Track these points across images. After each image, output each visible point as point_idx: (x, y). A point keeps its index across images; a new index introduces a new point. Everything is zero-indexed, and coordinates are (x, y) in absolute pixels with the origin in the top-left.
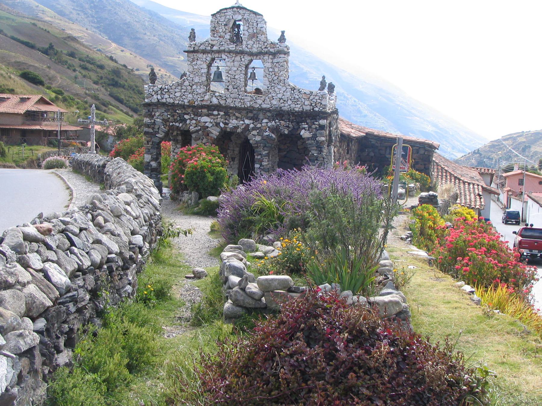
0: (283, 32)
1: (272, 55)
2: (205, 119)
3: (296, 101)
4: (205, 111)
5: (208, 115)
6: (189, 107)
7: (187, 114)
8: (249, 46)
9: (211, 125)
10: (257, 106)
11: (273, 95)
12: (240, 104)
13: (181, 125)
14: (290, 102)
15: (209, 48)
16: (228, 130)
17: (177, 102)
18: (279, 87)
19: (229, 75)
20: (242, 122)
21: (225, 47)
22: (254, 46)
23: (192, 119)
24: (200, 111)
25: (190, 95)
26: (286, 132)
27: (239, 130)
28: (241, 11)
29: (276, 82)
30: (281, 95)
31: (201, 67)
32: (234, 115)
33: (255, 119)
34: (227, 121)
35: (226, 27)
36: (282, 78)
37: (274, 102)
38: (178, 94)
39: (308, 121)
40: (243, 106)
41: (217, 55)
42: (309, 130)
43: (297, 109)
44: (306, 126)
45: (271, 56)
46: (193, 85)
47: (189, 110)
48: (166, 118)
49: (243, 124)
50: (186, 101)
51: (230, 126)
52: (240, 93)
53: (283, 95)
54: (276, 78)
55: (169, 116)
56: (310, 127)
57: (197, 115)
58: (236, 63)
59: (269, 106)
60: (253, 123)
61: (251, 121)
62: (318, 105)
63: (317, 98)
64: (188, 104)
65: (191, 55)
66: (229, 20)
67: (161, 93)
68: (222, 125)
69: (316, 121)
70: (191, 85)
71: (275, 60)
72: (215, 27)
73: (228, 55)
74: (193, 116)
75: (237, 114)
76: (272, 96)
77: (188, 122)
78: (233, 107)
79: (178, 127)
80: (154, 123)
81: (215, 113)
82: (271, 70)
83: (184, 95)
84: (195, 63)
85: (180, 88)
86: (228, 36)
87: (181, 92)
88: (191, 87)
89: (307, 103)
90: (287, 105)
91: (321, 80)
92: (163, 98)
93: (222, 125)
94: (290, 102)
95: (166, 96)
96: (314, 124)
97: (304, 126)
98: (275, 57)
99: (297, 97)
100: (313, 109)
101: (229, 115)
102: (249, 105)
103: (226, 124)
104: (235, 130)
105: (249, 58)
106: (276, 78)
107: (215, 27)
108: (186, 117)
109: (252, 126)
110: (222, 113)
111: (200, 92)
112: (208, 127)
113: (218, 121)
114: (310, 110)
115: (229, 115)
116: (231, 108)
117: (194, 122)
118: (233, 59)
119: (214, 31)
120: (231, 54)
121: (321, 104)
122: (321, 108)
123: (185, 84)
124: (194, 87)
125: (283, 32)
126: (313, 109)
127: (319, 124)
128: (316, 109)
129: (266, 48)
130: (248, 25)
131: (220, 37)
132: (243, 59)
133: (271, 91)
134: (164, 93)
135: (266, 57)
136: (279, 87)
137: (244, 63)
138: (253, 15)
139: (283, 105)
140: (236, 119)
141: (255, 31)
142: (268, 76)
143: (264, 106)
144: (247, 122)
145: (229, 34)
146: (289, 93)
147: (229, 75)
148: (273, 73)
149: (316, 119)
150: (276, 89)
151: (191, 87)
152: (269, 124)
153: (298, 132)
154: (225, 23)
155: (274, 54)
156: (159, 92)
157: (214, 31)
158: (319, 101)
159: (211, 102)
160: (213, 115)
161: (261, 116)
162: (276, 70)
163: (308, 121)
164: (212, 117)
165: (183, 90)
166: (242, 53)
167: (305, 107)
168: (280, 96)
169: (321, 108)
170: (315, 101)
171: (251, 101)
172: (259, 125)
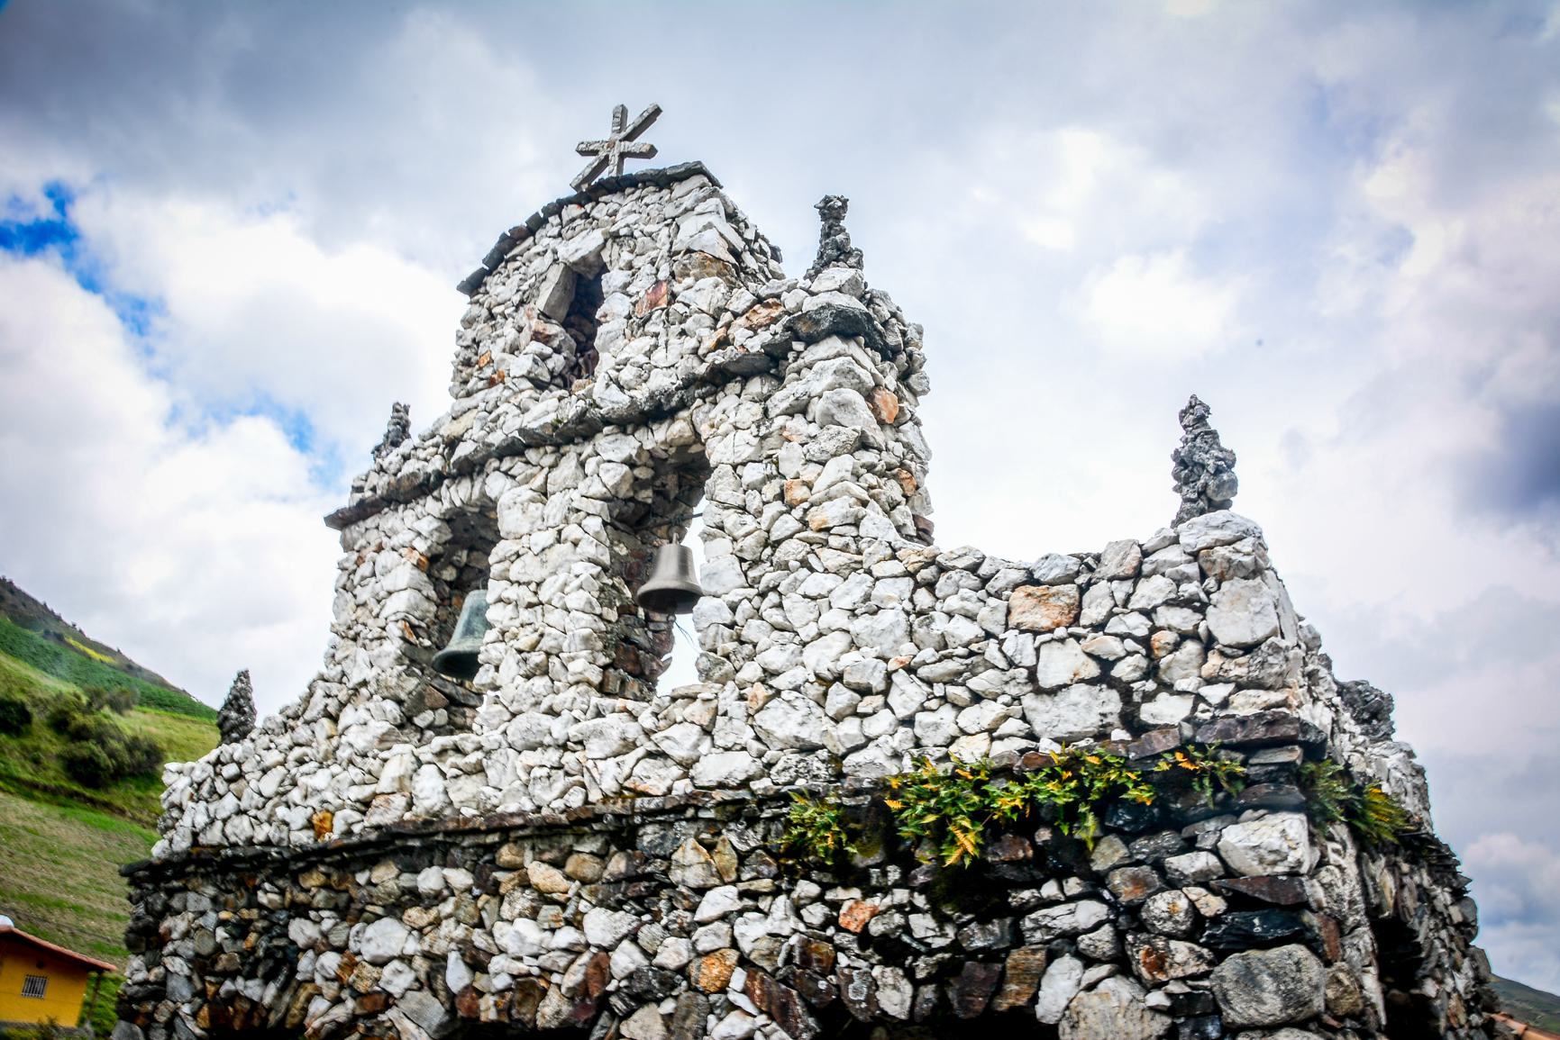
0: (832, 212)
1: (762, 373)
2: (385, 937)
3: (957, 677)
4: (386, 876)
5: (395, 908)
6: (310, 858)
7: (301, 910)
8: (627, 375)
9: (407, 979)
10: (658, 780)
11: (774, 658)
12: (560, 782)
13: (272, 989)
14: (908, 694)
15: (437, 464)
16: (488, 1010)
17: (260, 836)
18: (815, 583)
19: (512, 592)
20: (567, 936)
21: (511, 425)
22: (658, 356)
23: (317, 948)
24: (361, 878)
25: (321, 780)
26: (895, 998)
27: (552, 1009)
28: (600, 212)
29: (791, 550)
30: (838, 642)
31: (387, 583)
32: (525, 884)
33: (645, 891)
34: (479, 938)
35: (521, 318)
36: (831, 513)
37: (784, 721)
38: (269, 785)
39: (1107, 854)
40: (575, 799)
41: (458, 494)
42: (1122, 965)
43: (971, 751)
44: (1090, 912)
45: (756, 386)
46: (342, 705)
47: (313, 880)
48: (207, 948)
49: (573, 951)
50: (297, 817)
51: (500, 973)
52: (556, 701)
53: (854, 645)
54: (789, 523)
55: (221, 933)
56: (1129, 918)
57: (349, 912)
58: (556, 505)
59: (741, 765)
60: (633, 937)
61: (624, 921)
62: (1184, 667)
63: (1152, 590)
64: (305, 838)
65: (355, 531)
66: (542, 277)
67: (213, 791)
68: (456, 975)
69: (1190, 845)
70: (331, 709)
71: (781, 399)
72: (476, 342)
73: (519, 468)
74: (327, 925)
75: (540, 874)
76: (769, 674)
77: (304, 963)
78: (521, 814)
79: (255, 1005)
80: (158, 991)
81: (429, 880)
82: (752, 473)
83: (295, 784)
84: (365, 569)
85: (285, 741)
86: (520, 365)
87: (283, 764)
88: (335, 719)
89: (1061, 663)
90: (880, 724)
91: (1175, 437)
92: (212, 821)
93: (456, 975)
94: (908, 694)
95: (229, 803)
96: (1172, 882)
97: (1061, 918)
98: (780, 379)
99: (964, 631)
100: (1130, 720)
101: (494, 890)
102: (609, 785)
103: (477, 963)
104: (524, 1013)
105: (628, 446)
106: (789, 523)
107: (476, 342)
108: (301, 931)
109: (625, 960)
110: (461, 878)
111: (360, 744)
112: (388, 1001)
113: (440, 947)
114: (1102, 735)
115: (494, 890)
116: (505, 830)
117: (331, 961)
118: (539, 481)
119: (467, 363)
120: (531, 455)
121: (1209, 643)
122: (1215, 693)
123: (308, 716)
124: (347, 717)
125: (832, 212)
126: (1130, 720)
127: (1225, 878)
128: (1166, 711)
129: (723, 343)
130: (626, 256)
131: (491, 383)
132: (590, 466)
133: (752, 630)
134: (221, 786)
135: (728, 400)
136: (815, 583)
137: (597, 489)
138: (657, 196)
139: (850, 727)
140: (534, 914)
141: (663, 274)
142: (731, 519)
143: (713, 768)
144: (601, 925)
145: (537, 347)
146: (892, 617)
147: (512, 592)
148: (771, 490)
149: (1176, 822)
150: (798, 612)
151: (335, 719)
152: (752, 931)
153: (1014, 994)
154: (516, 299)
155: (772, 364)
156: (206, 788)
157: (467, 363)
158: (1182, 619)
159: (410, 805)
160: (414, 897)
161: (690, 864)
162: (791, 460)
163: (1107, 854)
164: (414, 914)
165: (297, 752)
166: (584, 429)
167: (1044, 714)
168: (821, 657)
169: (1215, 693)
170: (1139, 625)
171: (629, 746)
172: (673, 953)
